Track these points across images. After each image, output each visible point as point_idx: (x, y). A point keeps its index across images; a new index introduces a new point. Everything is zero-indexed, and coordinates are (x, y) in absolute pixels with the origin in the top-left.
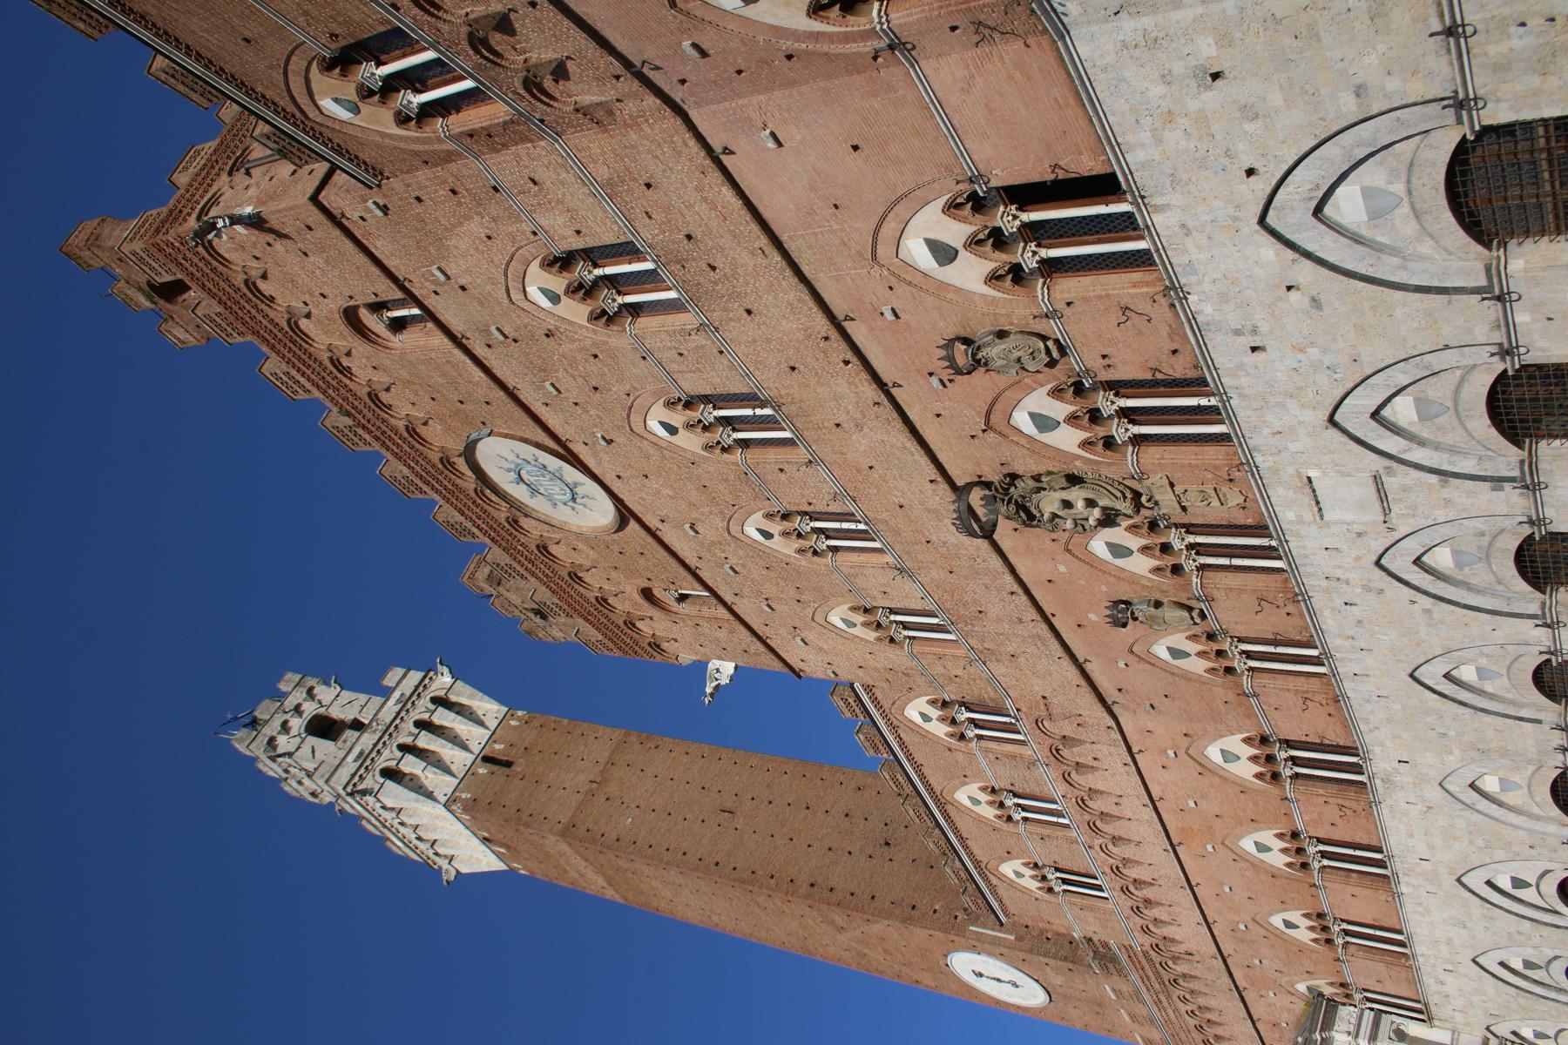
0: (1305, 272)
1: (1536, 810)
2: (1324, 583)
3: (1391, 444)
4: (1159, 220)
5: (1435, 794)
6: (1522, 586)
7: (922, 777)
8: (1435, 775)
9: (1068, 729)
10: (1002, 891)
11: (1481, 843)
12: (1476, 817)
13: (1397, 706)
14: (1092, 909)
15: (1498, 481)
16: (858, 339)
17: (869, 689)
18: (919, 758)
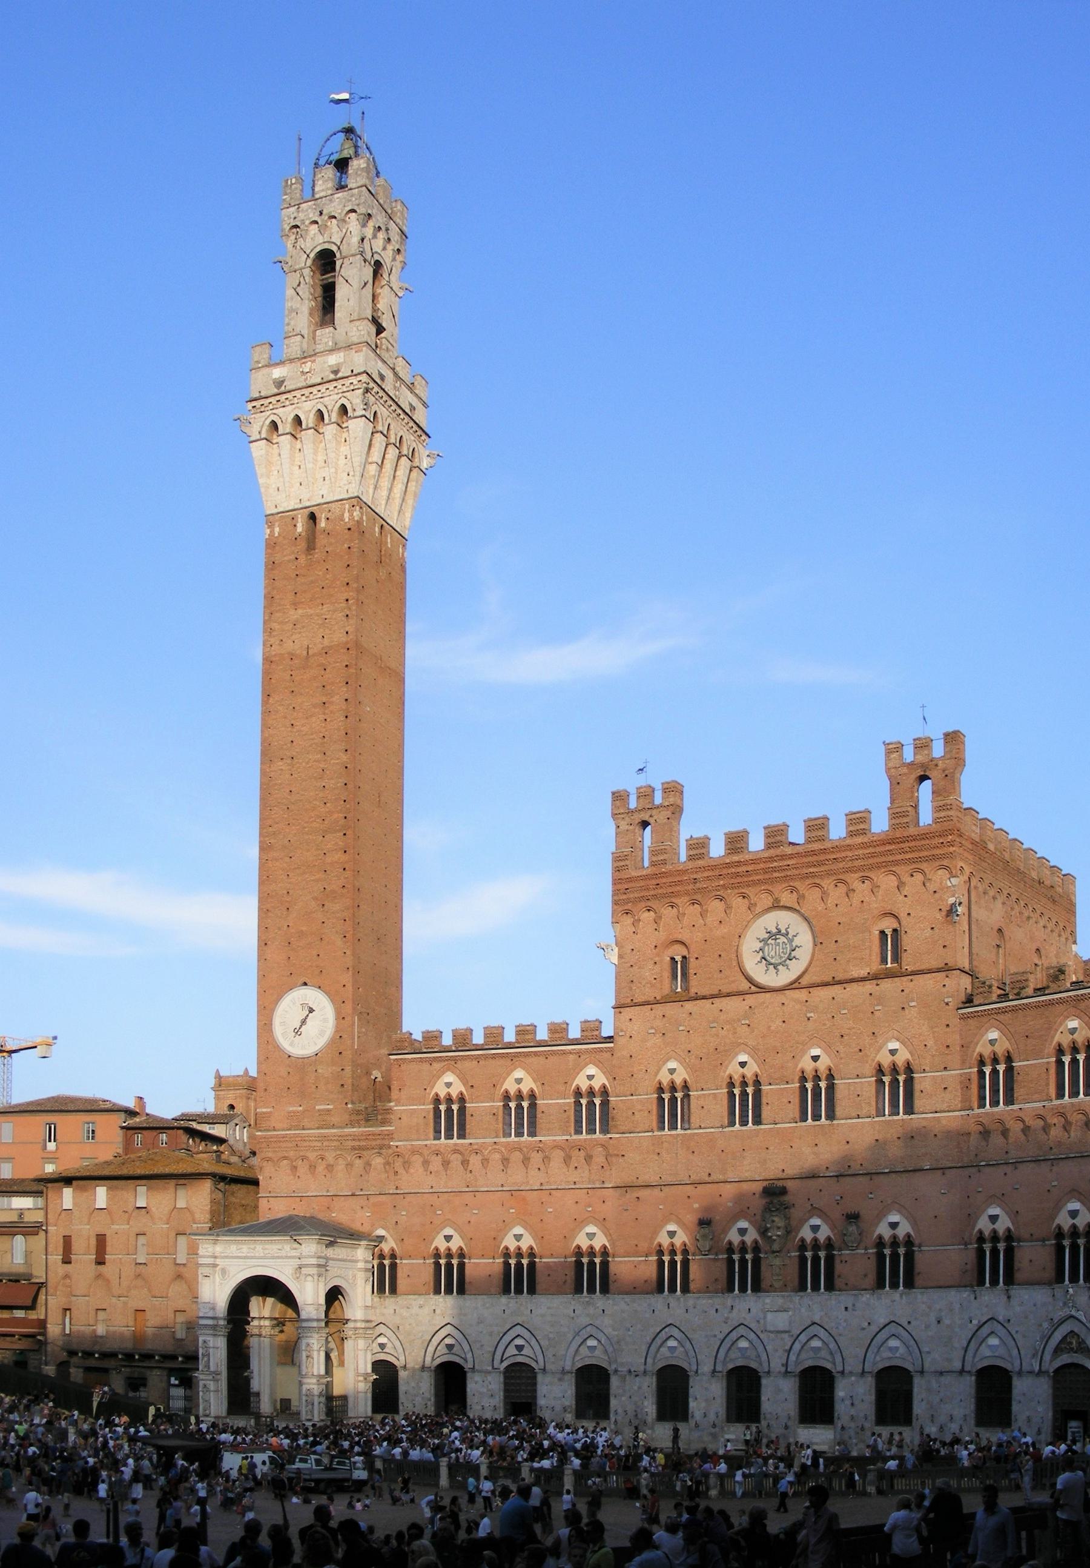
0: (874, 1329)
1: (577, 1358)
2: (729, 1304)
3: (803, 1338)
4: (896, 1295)
5: (585, 1321)
6: (731, 1366)
7: (536, 1054)
8: (597, 1323)
9: (599, 1159)
10: (425, 1066)
11: (551, 1336)
12: (570, 1336)
13: (647, 1315)
14: (427, 1124)
15: (786, 1365)
16: (861, 1179)
17: (610, 1050)
18: (553, 1059)
